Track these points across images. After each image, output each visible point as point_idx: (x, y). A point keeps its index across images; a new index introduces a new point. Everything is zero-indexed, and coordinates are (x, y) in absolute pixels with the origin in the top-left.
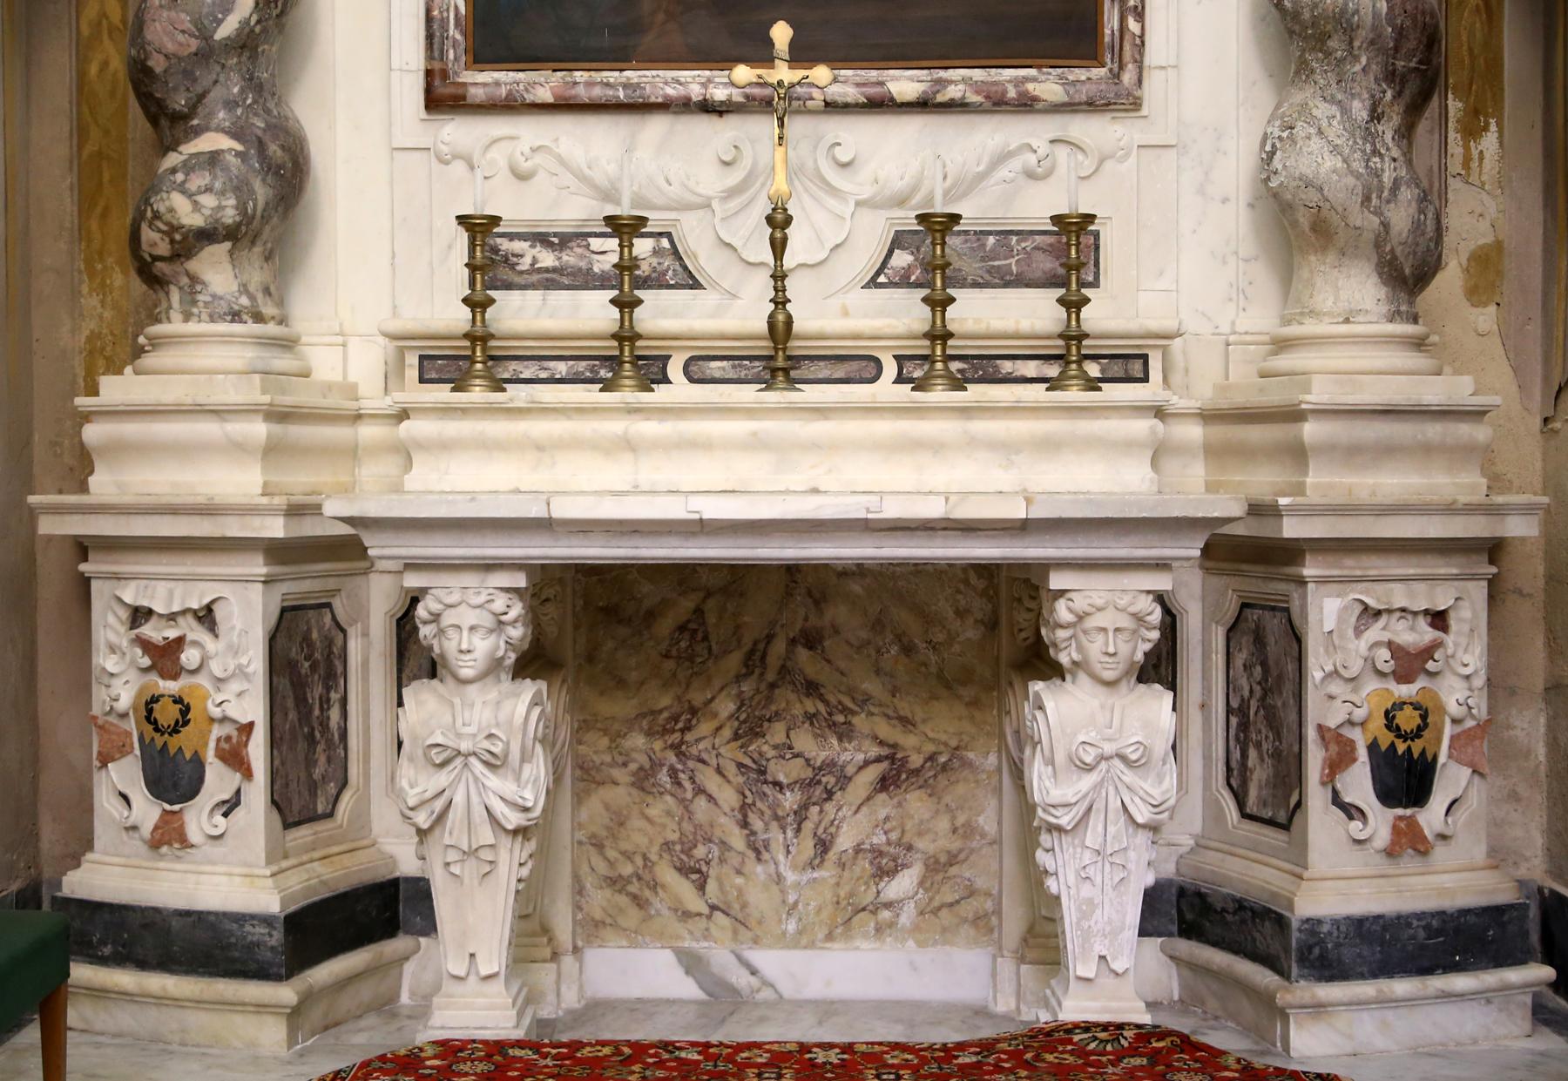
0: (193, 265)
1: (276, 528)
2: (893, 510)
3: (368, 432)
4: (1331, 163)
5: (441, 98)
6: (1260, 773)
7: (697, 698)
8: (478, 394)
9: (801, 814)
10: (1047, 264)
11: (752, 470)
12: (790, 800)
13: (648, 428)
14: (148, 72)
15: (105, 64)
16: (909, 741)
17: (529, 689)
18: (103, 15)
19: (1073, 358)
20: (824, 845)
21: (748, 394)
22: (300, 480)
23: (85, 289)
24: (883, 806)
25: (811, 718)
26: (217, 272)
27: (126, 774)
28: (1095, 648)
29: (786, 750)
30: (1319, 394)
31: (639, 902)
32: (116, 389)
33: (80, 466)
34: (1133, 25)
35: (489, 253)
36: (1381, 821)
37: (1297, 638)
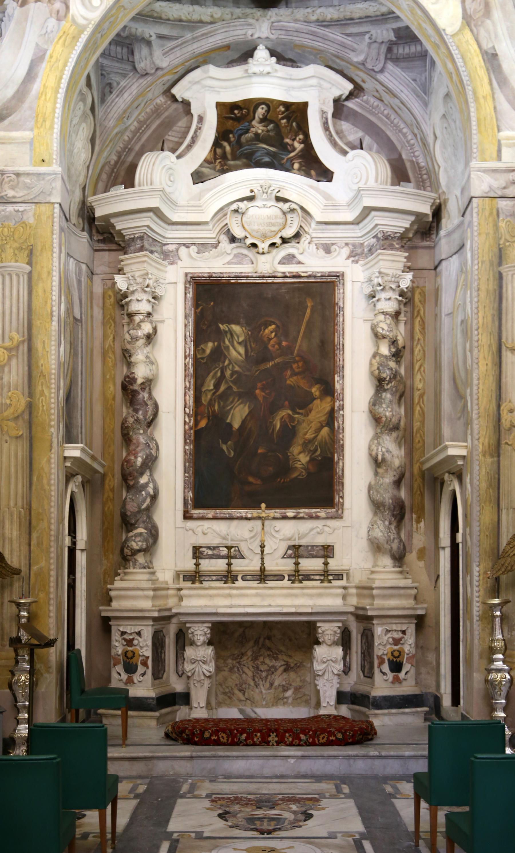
0: (136, 557)
1: (156, 614)
2: (285, 610)
3: (171, 592)
4: (380, 534)
5: (187, 516)
6: (367, 667)
7: (243, 651)
8: (197, 585)
9: (266, 677)
10: (322, 553)
11: (257, 601)
12: (264, 674)
13: (235, 592)
14: (126, 515)
15: (109, 508)
16: (291, 661)
17: (211, 648)
18: (108, 496)
19: (326, 575)
20: (271, 685)
21: (255, 584)
22: (160, 603)
23: (103, 559)
24: (285, 676)
25: (269, 656)
26: (141, 559)
27: (120, 668)
28: (326, 638)
29: (263, 663)
30: (377, 584)
31: (230, 698)
32: (118, 584)
33: (110, 600)
34: (341, 500)
35: (197, 552)
36: (391, 676)
37: (373, 636)
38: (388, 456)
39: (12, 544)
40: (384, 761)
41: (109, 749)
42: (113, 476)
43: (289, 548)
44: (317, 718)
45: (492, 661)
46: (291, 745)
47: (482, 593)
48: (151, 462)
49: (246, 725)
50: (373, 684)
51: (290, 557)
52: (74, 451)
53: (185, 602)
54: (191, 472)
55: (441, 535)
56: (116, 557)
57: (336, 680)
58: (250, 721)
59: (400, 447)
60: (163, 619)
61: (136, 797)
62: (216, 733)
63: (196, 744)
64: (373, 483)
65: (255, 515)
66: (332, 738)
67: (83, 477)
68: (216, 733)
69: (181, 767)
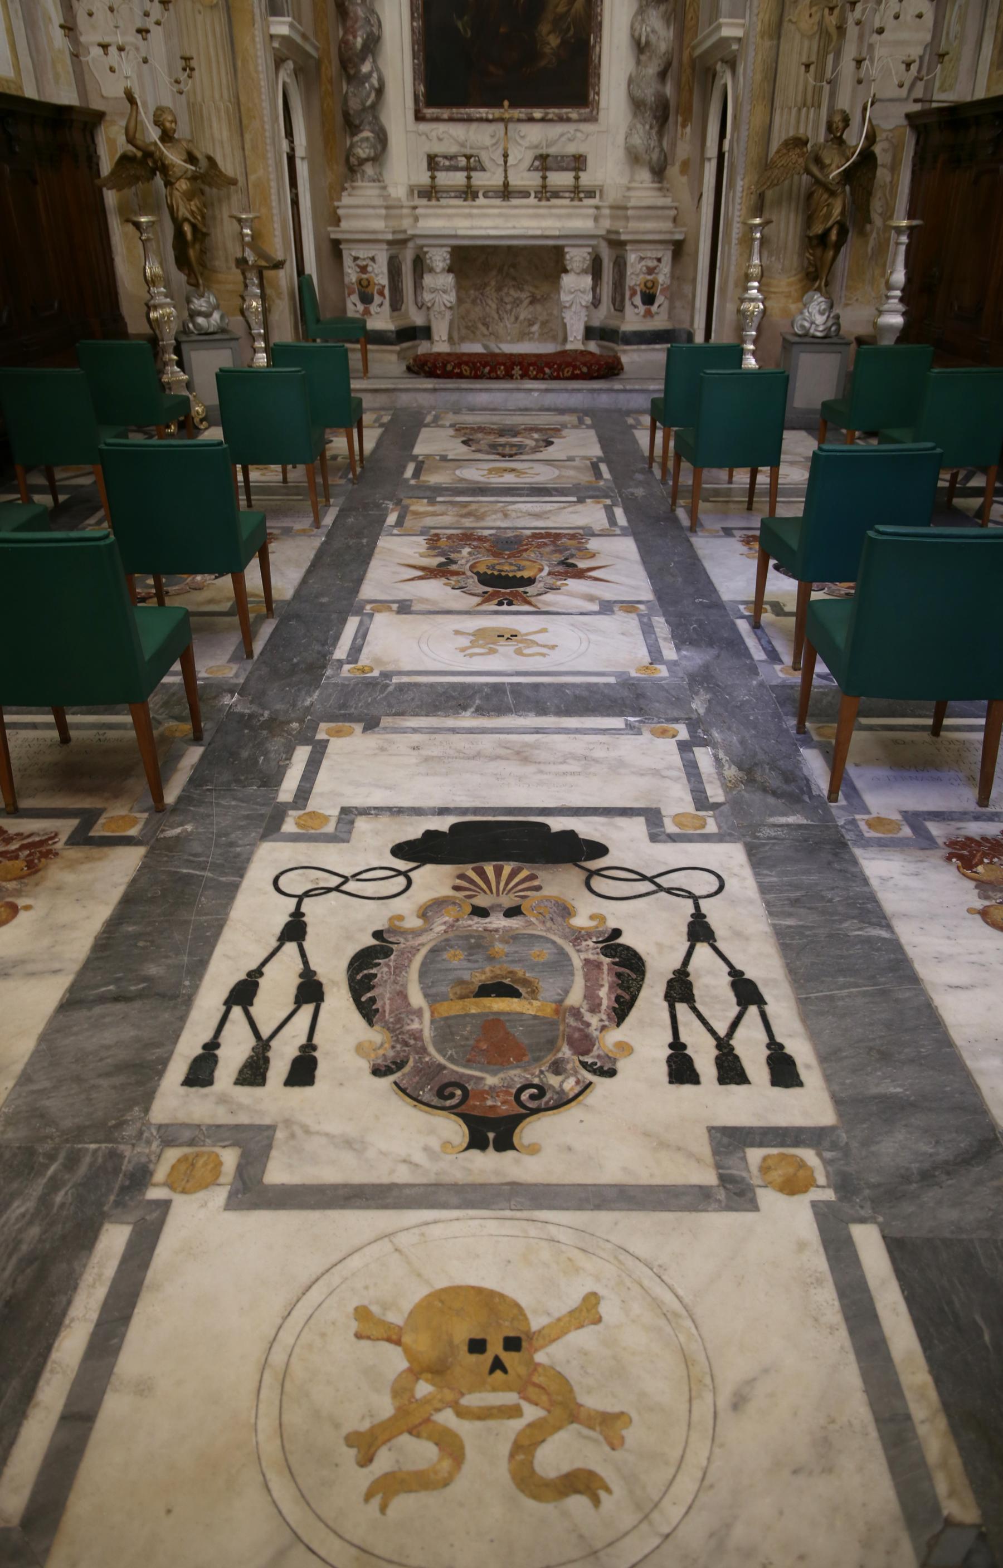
0: (363, 167)
1: (390, 237)
2: (531, 233)
3: (405, 211)
5: (419, 117)
8: (434, 202)
9: (511, 310)
10: (573, 165)
11: (500, 222)
12: (509, 307)
13: (475, 211)
14: (349, 114)
16: (537, 292)
19: (577, 192)
20: (517, 318)
21: (498, 202)
22: (394, 224)
24: (531, 308)
25: (514, 286)
27: (355, 298)
29: (508, 294)
30: (632, 203)
31: (473, 332)
32: (346, 200)
33: (337, 220)
34: (596, 97)
35: (433, 163)
36: (642, 309)
37: (625, 264)
38: (653, 38)
39: (223, 147)
40: (629, 395)
41: (352, 381)
42: (330, 62)
43: (536, 158)
44: (564, 353)
45: (747, 289)
46: (535, 378)
47: (744, 212)
48: (373, 44)
49: (489, 359)
50: (623, 317)
51: (537, 169)
52: (281, 27)
53: (422, 223)
54: (421, 58)
55: (709, 143)
56: (341, 168)
57: (583, 313)
58: (494, 355)
59: (668, 28)
60: (398, 243)
61: (381, 425)
62: (459, 365)
63: (438, 377)
64: (633, 75)
65: (497, 115)
66: (577, 372)
67: (295, 63)
68: (459, 365)
69: (425, 400)
